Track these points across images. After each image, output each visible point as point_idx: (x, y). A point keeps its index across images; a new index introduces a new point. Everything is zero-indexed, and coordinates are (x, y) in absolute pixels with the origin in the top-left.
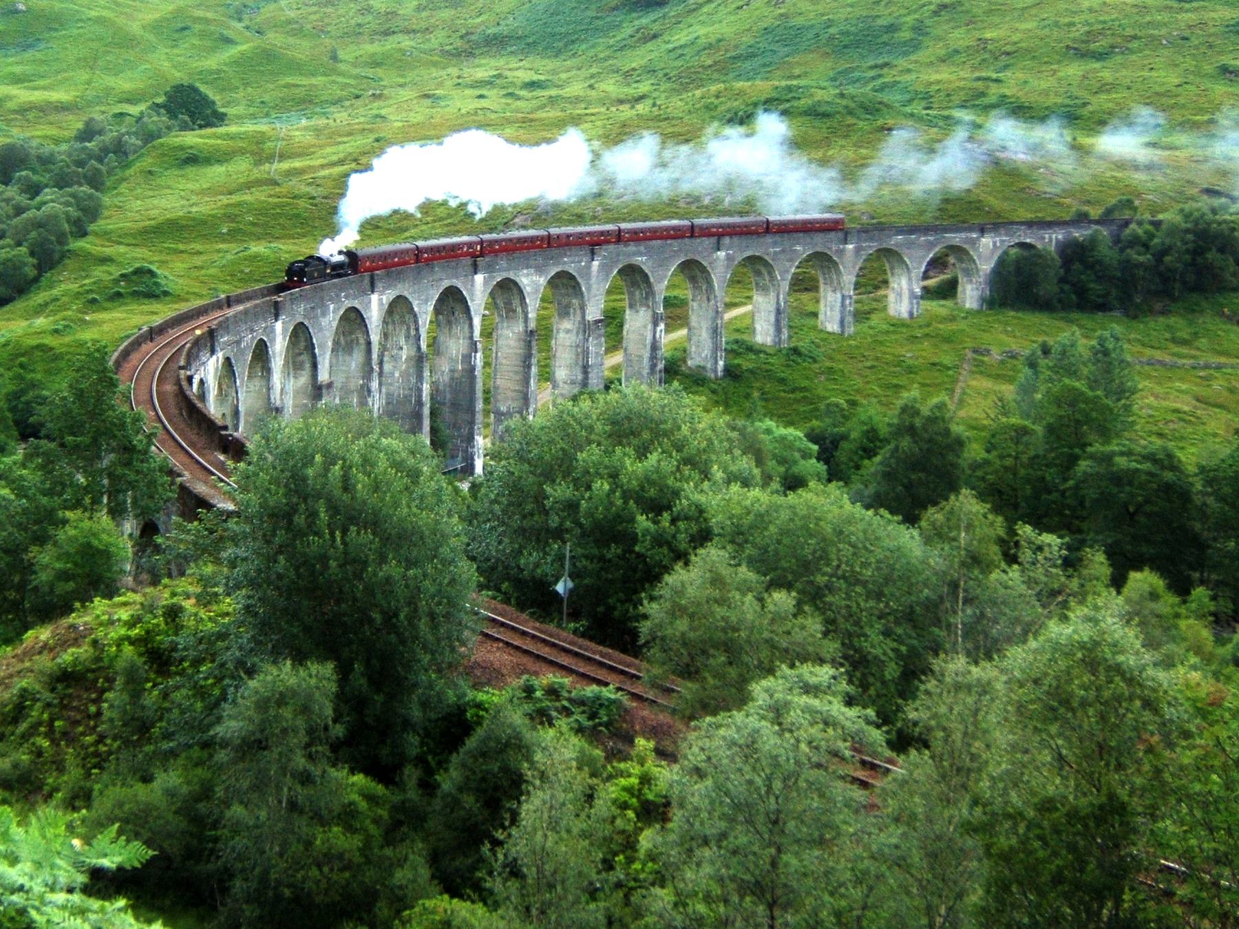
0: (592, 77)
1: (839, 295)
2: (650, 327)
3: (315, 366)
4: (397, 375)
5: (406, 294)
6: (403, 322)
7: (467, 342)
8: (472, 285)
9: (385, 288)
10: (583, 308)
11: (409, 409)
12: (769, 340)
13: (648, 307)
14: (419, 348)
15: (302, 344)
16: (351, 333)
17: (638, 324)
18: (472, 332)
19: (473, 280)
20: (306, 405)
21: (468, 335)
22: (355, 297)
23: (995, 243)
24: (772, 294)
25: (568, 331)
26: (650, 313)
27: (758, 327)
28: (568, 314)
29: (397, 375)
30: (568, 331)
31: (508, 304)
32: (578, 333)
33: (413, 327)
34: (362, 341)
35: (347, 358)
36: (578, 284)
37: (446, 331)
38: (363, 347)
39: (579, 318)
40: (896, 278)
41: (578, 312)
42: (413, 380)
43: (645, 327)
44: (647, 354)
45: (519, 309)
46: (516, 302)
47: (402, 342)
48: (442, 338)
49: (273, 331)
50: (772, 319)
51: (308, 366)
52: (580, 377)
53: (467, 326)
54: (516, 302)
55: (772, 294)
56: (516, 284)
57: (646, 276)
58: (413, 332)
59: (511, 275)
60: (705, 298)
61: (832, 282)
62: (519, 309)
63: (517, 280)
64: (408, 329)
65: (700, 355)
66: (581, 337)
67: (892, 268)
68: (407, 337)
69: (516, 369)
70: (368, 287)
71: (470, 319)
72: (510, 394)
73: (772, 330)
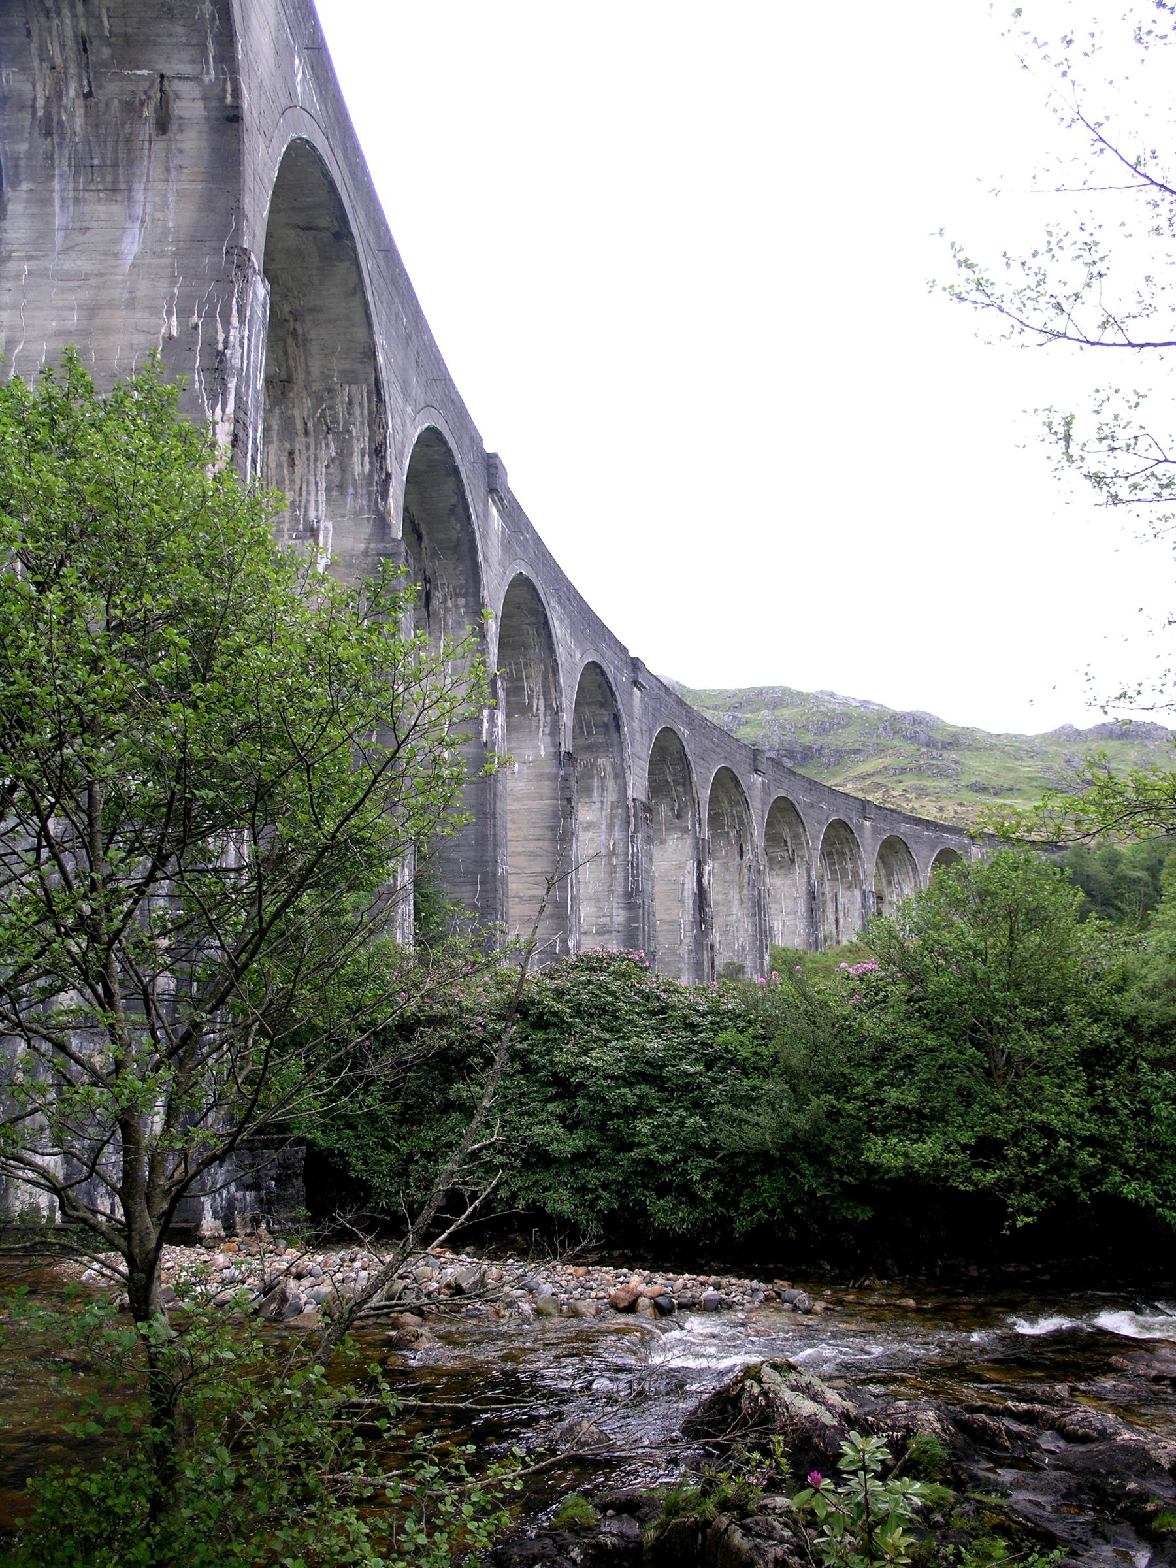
1: (857, 893)
2: (691, 866)
6: (328, 427)
10: (620, 775)
12: (798, 942)
13: (685, 830)
14: (382, 523)
25: (590, 826)
26: (689, 841)
27: (777, 925)
32: (610, 827)
33: (360, 444)
35: (100, 210)
36: (616, 718)
38: (192, 141)
39: (611, 796)
41: (611, 783)
43: (681, 866)
44: (687, 914)
45: (539, 704)
47: (318, 508)
50: (802, 908)
54: (533, 683)
55: (799, 871)
58: (360, 466)
61: (844, 874)
62: (539, 704)
64: (342, 458)
65: (729, 946)
66: (618, 834)
68: (338, 488)
69: (533, 846)
73: (802, 926)
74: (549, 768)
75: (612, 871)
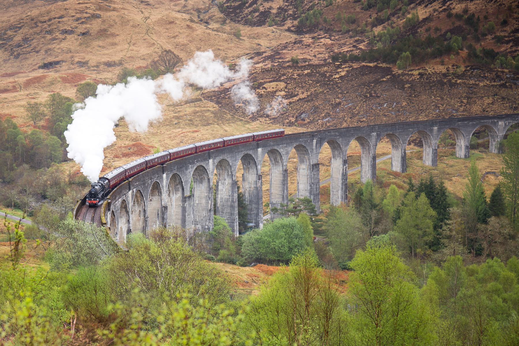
0: (356, 41)
2: (341, 166)
3: (183, 189)
4: (224, 190)
5: (226, 158)
7: (255, 175)
8: (257, 153)
9: (215, 157)
10: (309, 160)
11: (229, 203)
15: (178, 181)
16: (201, 175)
17: (336, 165)
18: (257, 172)
19: (257, 151)
20: (180, 205)
21: (256, 173)
22: (202, 161)
23: (505, 124)
24: (400, 150)
25: (304, 169)
28: (304, 162)
29: (224, 190)
30: (304, 169)
31: (275, 159)
32: (308, 170)
34: (206, 178)
35: (201, 185)
37: (247, 171)
38: (206, 180)
39: (308, 164)
40: (459, 141)
41: (308, 161)
42: (230, 193)
43: (340, 165)
44: (340, 177)
45: (280, 161)
46: (279, 158)
48: (245, 175)
49: (162, 178)
51: (180, 190)
52: (309, 188)
53: (255, 170)
54: (279, 158)
56: (278, 151)
57: (339, 145)
58: (230, 173)
59: (276, 148)
60: (368, 152)
63: (278, 150)
64: (228, 172)
66: (309, 171)
67: (457, 136)
68: (228, 175)
70: (208, 157)
71: (257, 167)
72: (277, 196)
74: (282, 172)
75: (308, 179)
